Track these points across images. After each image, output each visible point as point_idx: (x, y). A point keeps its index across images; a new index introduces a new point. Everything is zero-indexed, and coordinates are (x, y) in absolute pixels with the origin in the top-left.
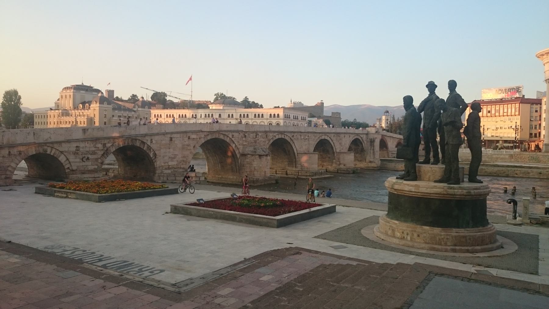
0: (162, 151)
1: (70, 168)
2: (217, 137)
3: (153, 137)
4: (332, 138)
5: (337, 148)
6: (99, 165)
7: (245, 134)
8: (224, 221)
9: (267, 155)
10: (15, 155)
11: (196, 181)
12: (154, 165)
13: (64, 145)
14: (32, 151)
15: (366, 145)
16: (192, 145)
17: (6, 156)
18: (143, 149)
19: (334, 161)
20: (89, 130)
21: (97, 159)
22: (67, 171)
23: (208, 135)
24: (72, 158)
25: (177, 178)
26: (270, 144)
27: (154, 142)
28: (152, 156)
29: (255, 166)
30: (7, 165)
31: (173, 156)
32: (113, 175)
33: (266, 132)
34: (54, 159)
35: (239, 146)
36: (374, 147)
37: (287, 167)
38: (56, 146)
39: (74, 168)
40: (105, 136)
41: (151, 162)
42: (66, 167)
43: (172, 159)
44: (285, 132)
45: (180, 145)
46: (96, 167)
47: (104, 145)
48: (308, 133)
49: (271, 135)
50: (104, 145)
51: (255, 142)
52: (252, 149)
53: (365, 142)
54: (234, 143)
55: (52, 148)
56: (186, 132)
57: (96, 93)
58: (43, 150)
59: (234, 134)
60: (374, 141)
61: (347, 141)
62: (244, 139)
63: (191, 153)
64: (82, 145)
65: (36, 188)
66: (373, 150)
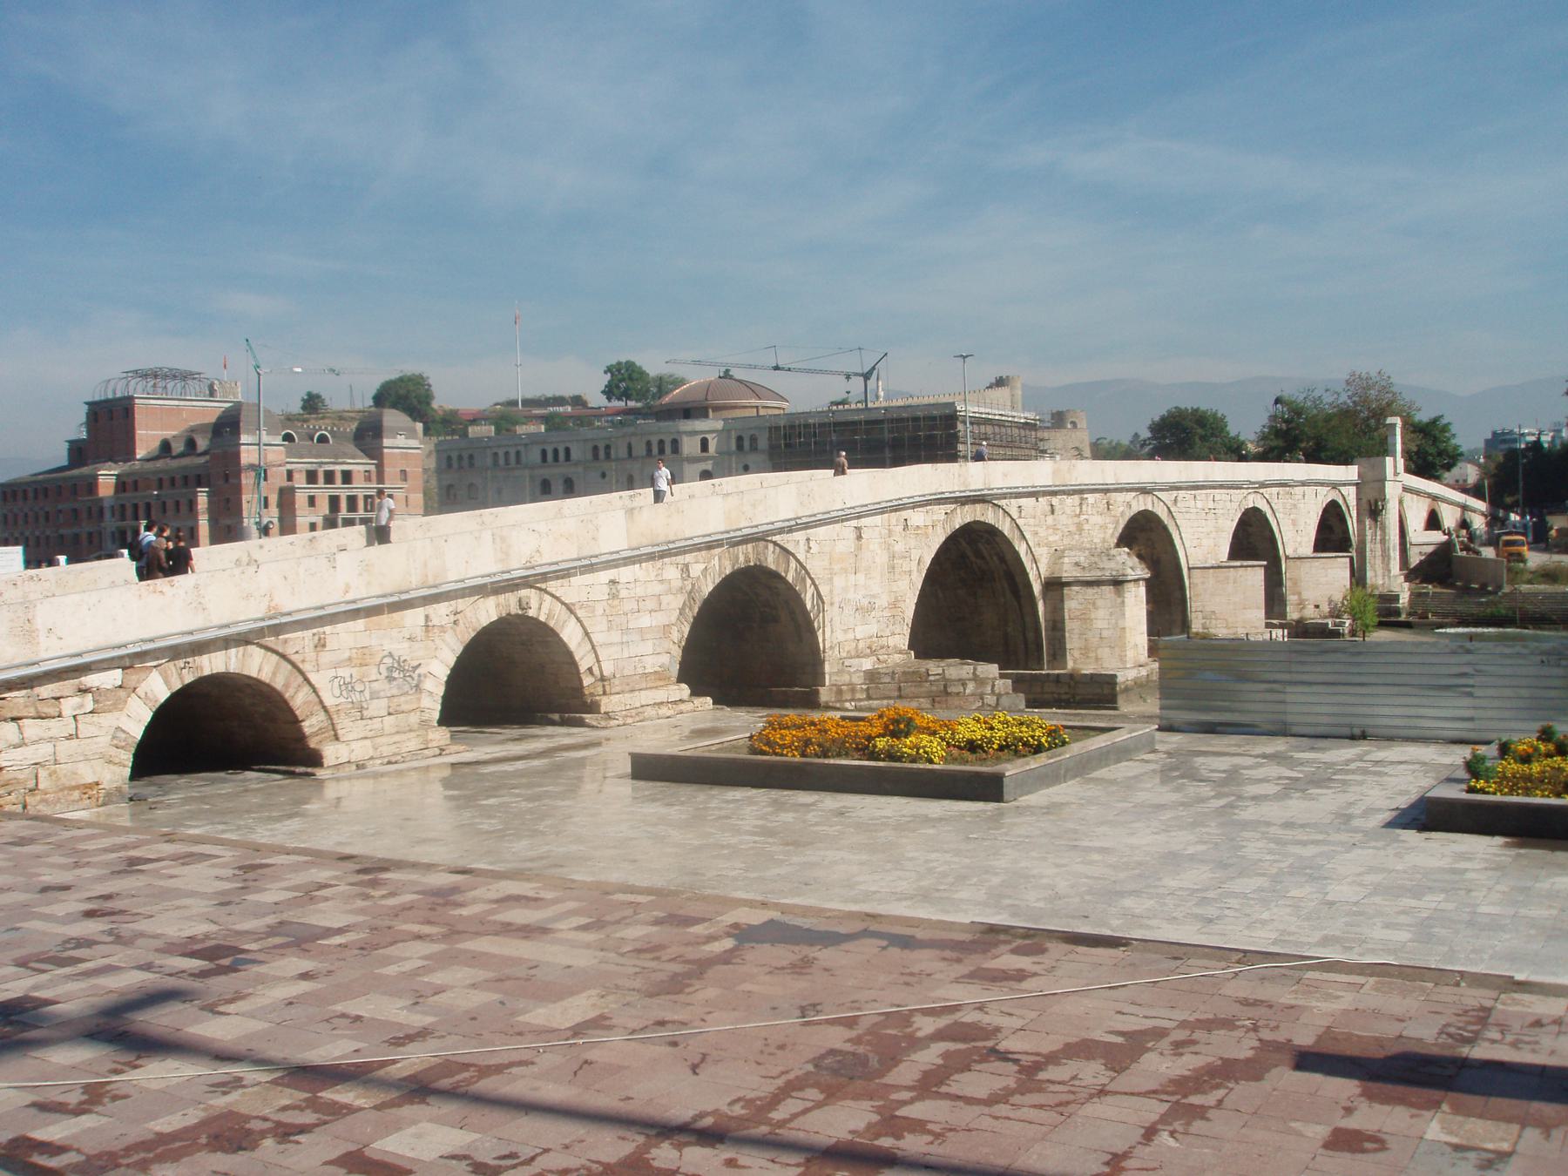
10: (442, 629)
14: (487, 612)
16: (915, 555)
17: (419, 632)
18: (783, 580)
21: (666, 628)
22: (587, 681)
27: (815, 547)
28: (809, 607)
29: (1099, 624)
31: (865, 602)
35: (1037, 551)
36: (1383, 529)
38: (552, 586)
42: (583, 668)
45: (882, 558)
46: (665, 659)
47: (686, 568)
59: (1023, 501)
62: (1050, 519)
64: (625, 574)
66: (1383, 541)
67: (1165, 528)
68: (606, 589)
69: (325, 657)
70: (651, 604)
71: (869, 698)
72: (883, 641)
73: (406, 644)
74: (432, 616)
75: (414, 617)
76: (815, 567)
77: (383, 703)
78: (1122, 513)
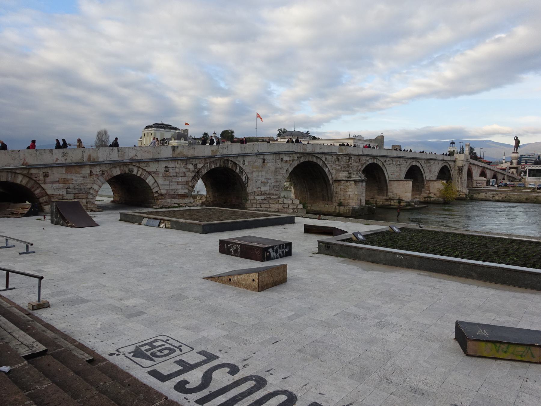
0: (255, 174)
1: (159, 192)
2: (310, 159)
3: (245, 158)
4: (423, 164)
5: (427, 176)
6: (191, 188)
7: (337, 156)
8: (431, 273)
9: (362, 181)
11: (293, 209)
12: (246, 190)
13: (151, 164)
14: (117, 172)
15: (454, 173)
16: (285, 168)
17: (87, 176)
18: (235, 172)
19: (423, 189)
20: (179, 148)
21: (187, 182)
23: (301, 157)
24: (160, 181)
25: (272, 206)
26: (362, 169)
28: (244, 180)
30: (88, 187)
31: (265, 181)
32: (201, 202)
33: (359, 155)
34: (141, 181)
35: (331, 171)
36: (462, 175)
37: (376, 196)
38: (143, 166)
39: (163, 192)
40: (196, 155)
41: (243, 187)
42: (154, 191)
43: (264, 183)
44: (377, 156)
46: (187, 191)
48: (400, 158)
49: (364, 159)
50: (195, 165)
51: (348, 166)
52: (346, 174)
53: (453, 170)
54: (327, 167)
55: (139, 167)
56: (279, 153)
57: (174, 131)
58: (129, 169)
59: (327, 156)
60: (462, 169)
61: (436, 168)
62: (337, 163)
63: (284, 177)
64: (171, 165)
65: (121, 214)
66: (461, 178)
67: (381, 169)
68: (164, 169)
69: (48, 180)
70: (181, 174)
71: (261, 207)
72: (272, 192)
75: (86, 171)
76: (246, 169)
77: (72, 195)
78: (365, 163)
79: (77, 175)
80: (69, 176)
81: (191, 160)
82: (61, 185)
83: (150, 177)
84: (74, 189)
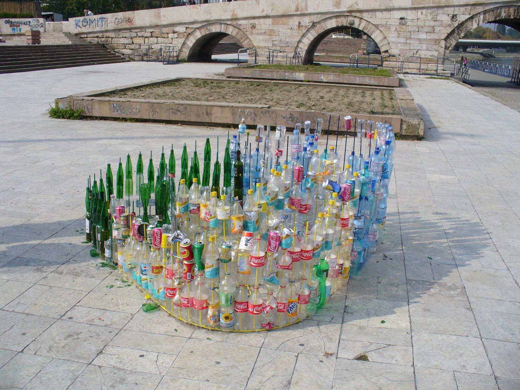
17: (296, 27)
24: (392, 37)
38: (365, 16)
46: (436, 54)
47: (454, 17)
64: (410, 15)
68: (398, 21)
69: (254, 31)
70: (426, 30)
73: (289, 31)
74: (302, 22)
75: (294, 22)
79: (284, 26)
80: (275, 28)
81: (446, 9)
82: (268, 37)
83: (378, 32)
84: (281, 41)
